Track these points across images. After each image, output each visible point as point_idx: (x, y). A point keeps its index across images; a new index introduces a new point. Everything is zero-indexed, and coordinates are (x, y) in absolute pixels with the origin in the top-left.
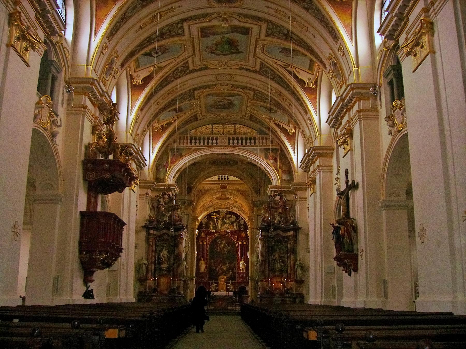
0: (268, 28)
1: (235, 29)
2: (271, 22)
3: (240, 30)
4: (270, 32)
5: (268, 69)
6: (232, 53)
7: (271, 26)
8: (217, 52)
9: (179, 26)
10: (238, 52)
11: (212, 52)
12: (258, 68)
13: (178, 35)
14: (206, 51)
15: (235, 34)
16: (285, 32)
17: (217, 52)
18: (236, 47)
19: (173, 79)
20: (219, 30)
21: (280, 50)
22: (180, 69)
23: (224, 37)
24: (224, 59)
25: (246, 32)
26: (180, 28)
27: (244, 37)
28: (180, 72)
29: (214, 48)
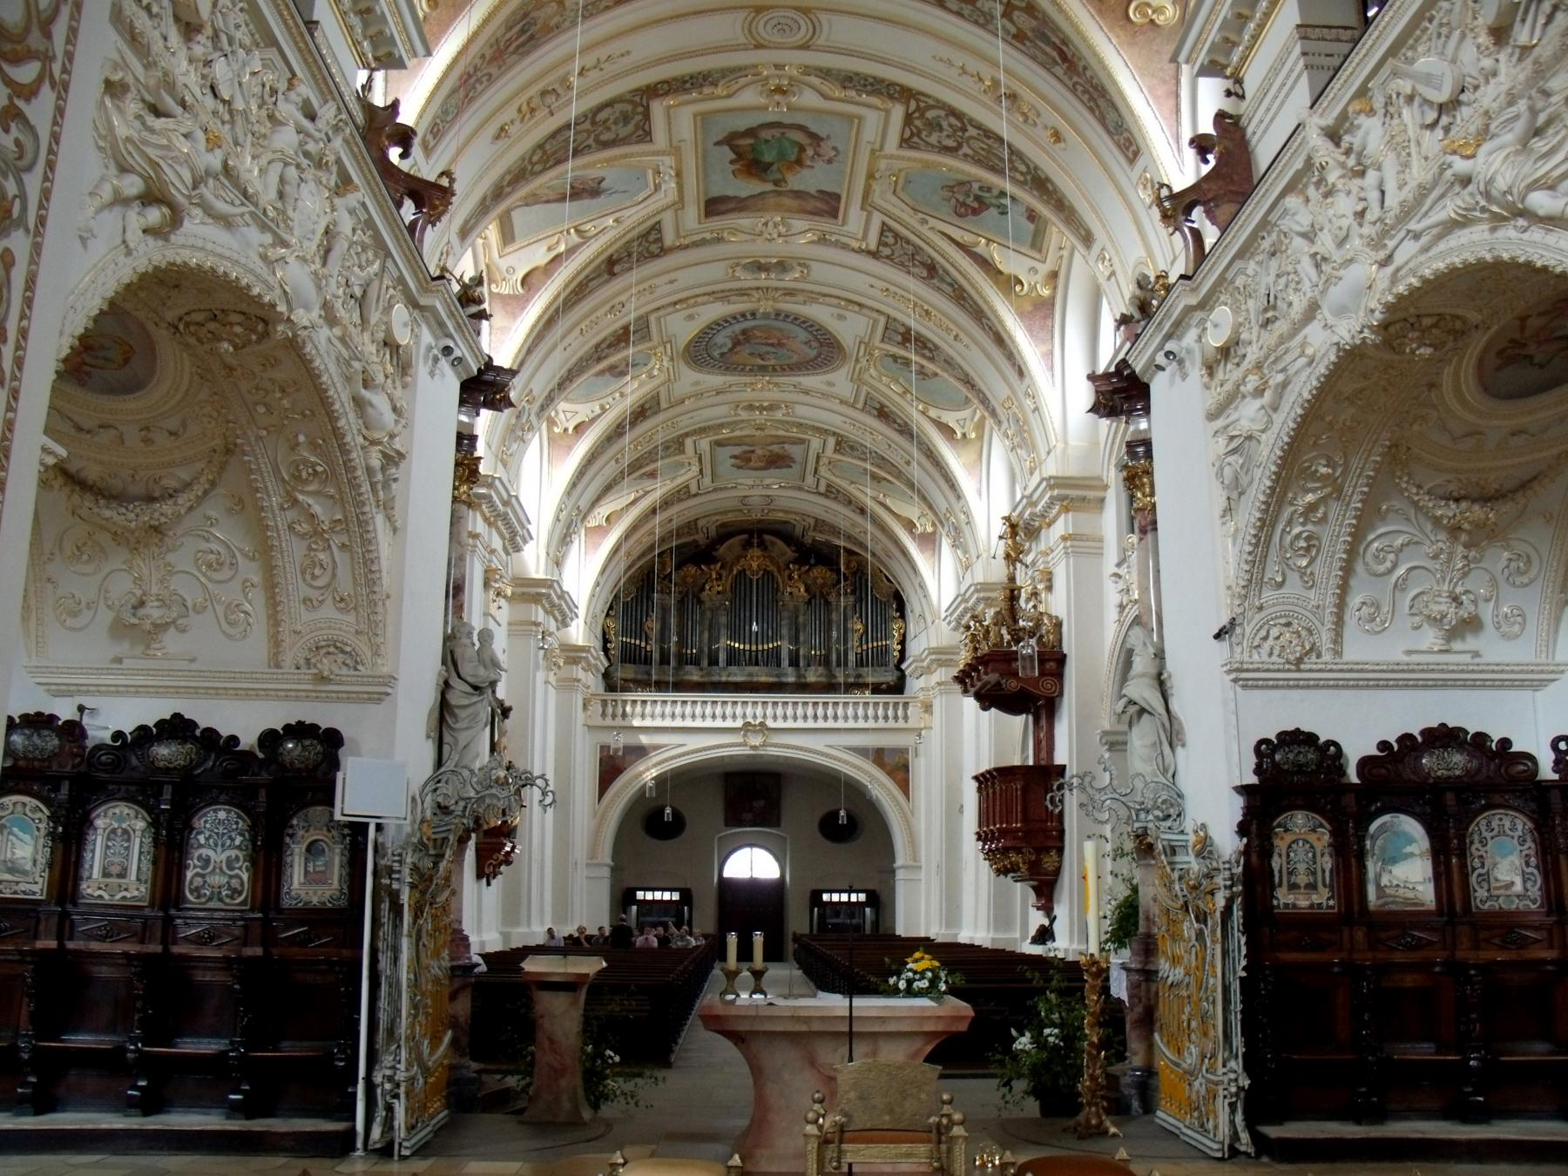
0: (660, 240)
1: (740, 205)
2: (657, 256)
3: (731, 206)
4: (651, 238)
5: (624, 131)
6: (751, 132)
7: (654, 248)
8: (798, 136)
9: (887, 251)
10: (730, 140)
11: (816, 138)
12: (657, 108)
13: (897, 235)
14: (834, 148)
15: (744, 194)
16: (617, 269)
17: (798, 136)
18: (739, 155)
19: (972, 132)
20: (787, 201)
21: (603, 185)
22: (933, 139)
23: (776, 183)
24: (776, 111)
25: (714, 206)
26: (886, 245)
27: (716, 192)
28: (941, 129)
29: (810, 152)
